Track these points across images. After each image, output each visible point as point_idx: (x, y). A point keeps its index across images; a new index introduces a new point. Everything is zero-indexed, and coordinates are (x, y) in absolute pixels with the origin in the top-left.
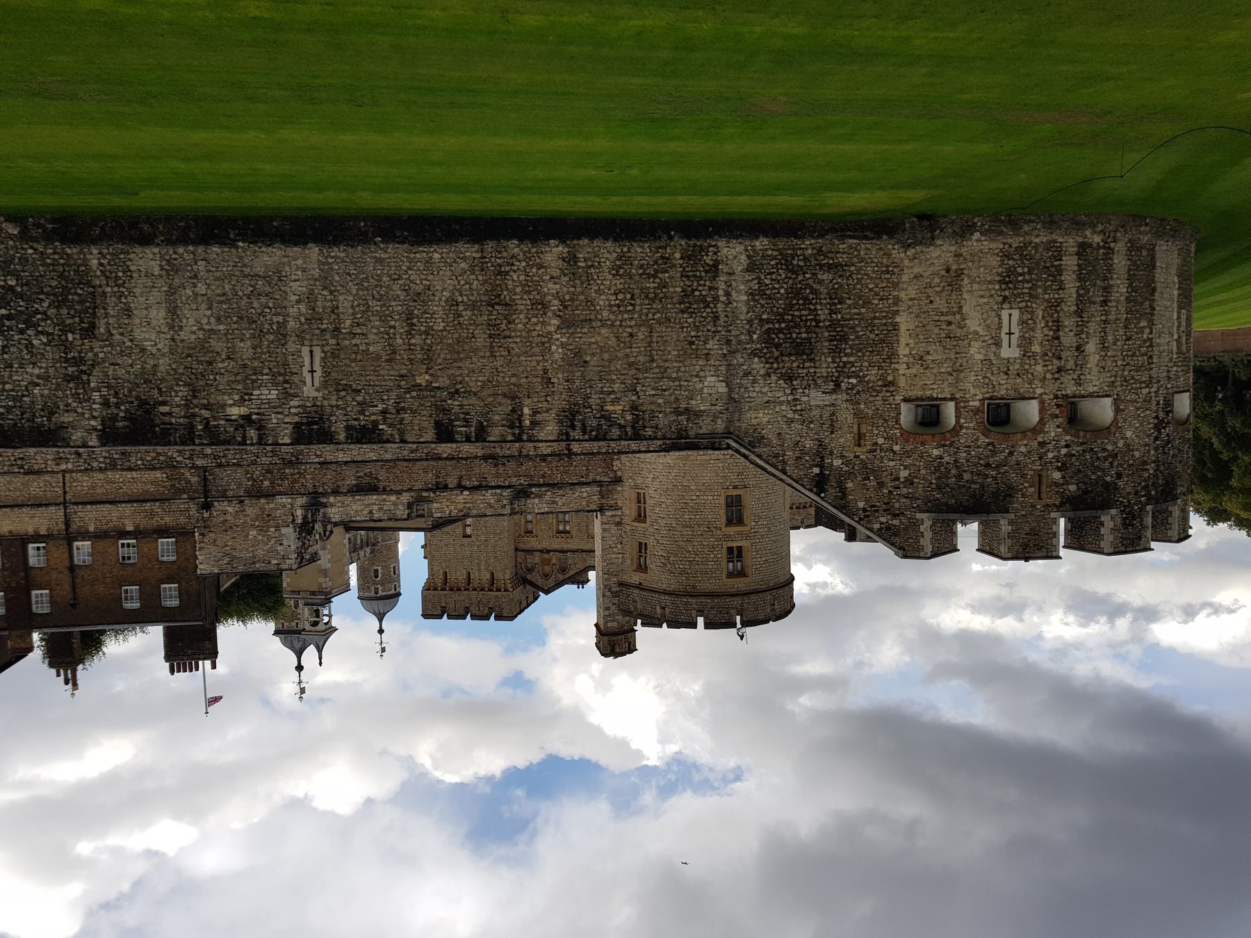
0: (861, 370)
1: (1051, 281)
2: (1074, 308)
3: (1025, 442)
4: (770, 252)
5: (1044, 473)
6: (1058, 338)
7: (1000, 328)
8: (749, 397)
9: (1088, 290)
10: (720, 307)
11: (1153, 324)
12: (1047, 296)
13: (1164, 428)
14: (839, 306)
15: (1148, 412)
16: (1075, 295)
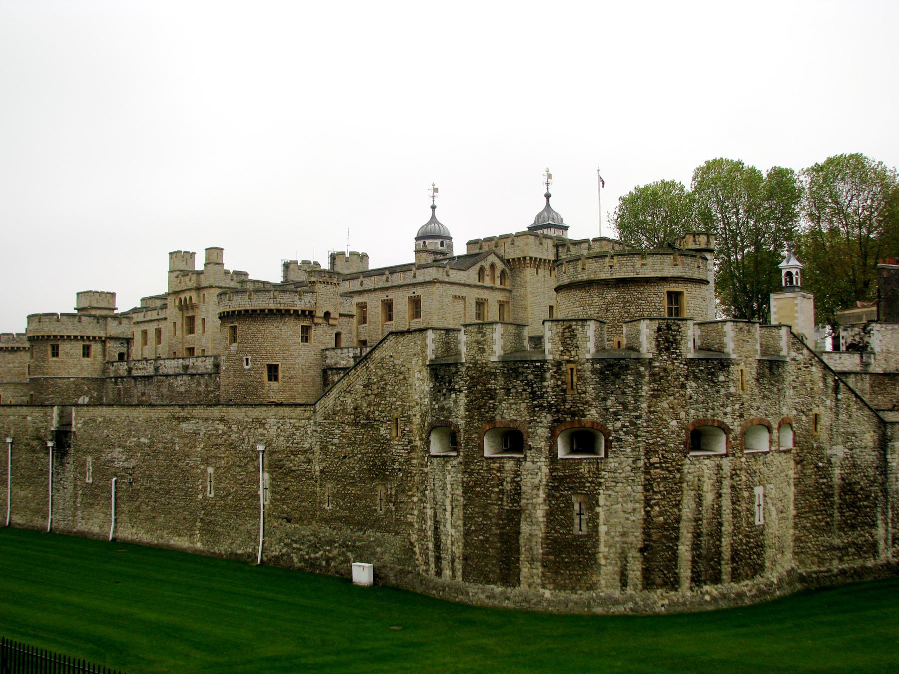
0: (816, 472)
1: (739, 550)
2: (723, 529)
3: (751, 417)
4: (866, 556)
5: (741, 391)
6: (733, 503)
7: (764, 509)
8: (874, 451)
9: (714, 543)
10: (890, 515)
11: (645, 520)
12: (740, 536)
13: (623, 426)
14: (828, 520)
15: (651, 441)
16: (723, 540)
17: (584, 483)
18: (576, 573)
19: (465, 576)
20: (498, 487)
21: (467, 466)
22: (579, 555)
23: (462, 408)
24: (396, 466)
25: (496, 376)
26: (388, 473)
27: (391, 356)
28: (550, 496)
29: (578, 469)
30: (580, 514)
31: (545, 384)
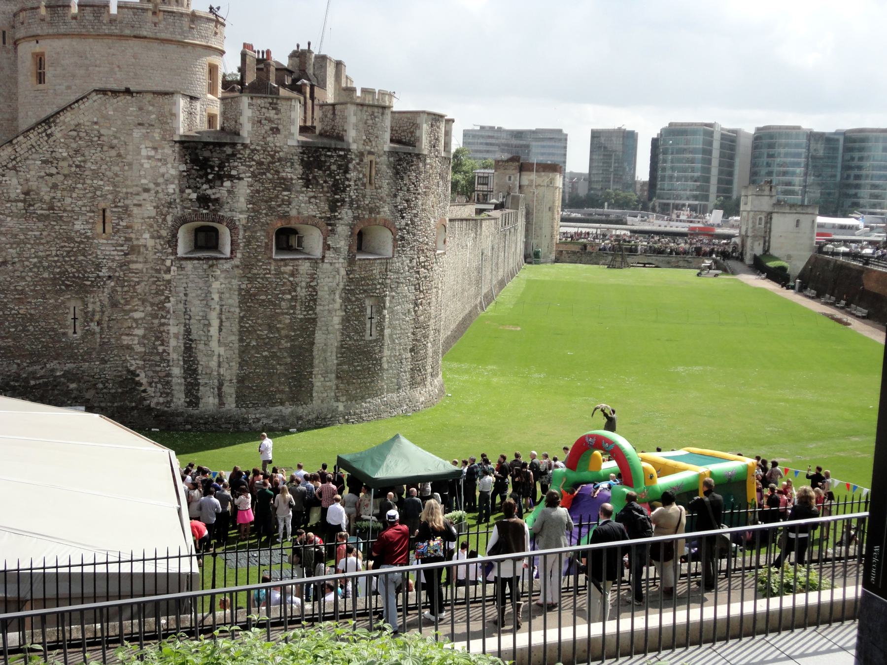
13: (407, 225)
17: (375, 284)
18: (365, 380)
19: (241, 399)
20: (290, 293)
21: (247, 271)
22: (369, 361)
23: (242, 199)
24: (104, 272)
25: (292, 164)
26: (88, 283)
27: (96, 123)
28: (346, 300)
29: (372, 270)
30: (371, 318)
31: (348, 176)
